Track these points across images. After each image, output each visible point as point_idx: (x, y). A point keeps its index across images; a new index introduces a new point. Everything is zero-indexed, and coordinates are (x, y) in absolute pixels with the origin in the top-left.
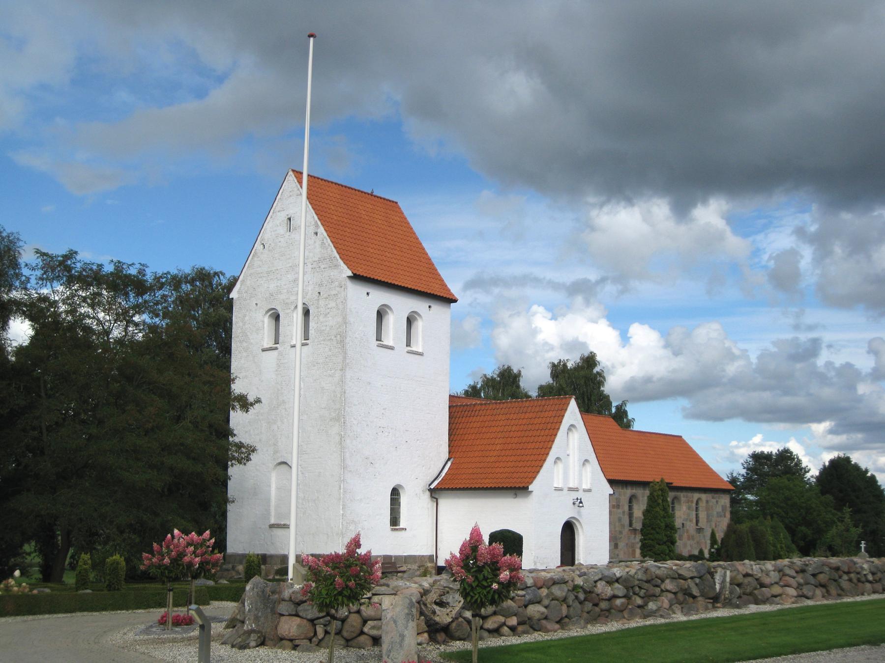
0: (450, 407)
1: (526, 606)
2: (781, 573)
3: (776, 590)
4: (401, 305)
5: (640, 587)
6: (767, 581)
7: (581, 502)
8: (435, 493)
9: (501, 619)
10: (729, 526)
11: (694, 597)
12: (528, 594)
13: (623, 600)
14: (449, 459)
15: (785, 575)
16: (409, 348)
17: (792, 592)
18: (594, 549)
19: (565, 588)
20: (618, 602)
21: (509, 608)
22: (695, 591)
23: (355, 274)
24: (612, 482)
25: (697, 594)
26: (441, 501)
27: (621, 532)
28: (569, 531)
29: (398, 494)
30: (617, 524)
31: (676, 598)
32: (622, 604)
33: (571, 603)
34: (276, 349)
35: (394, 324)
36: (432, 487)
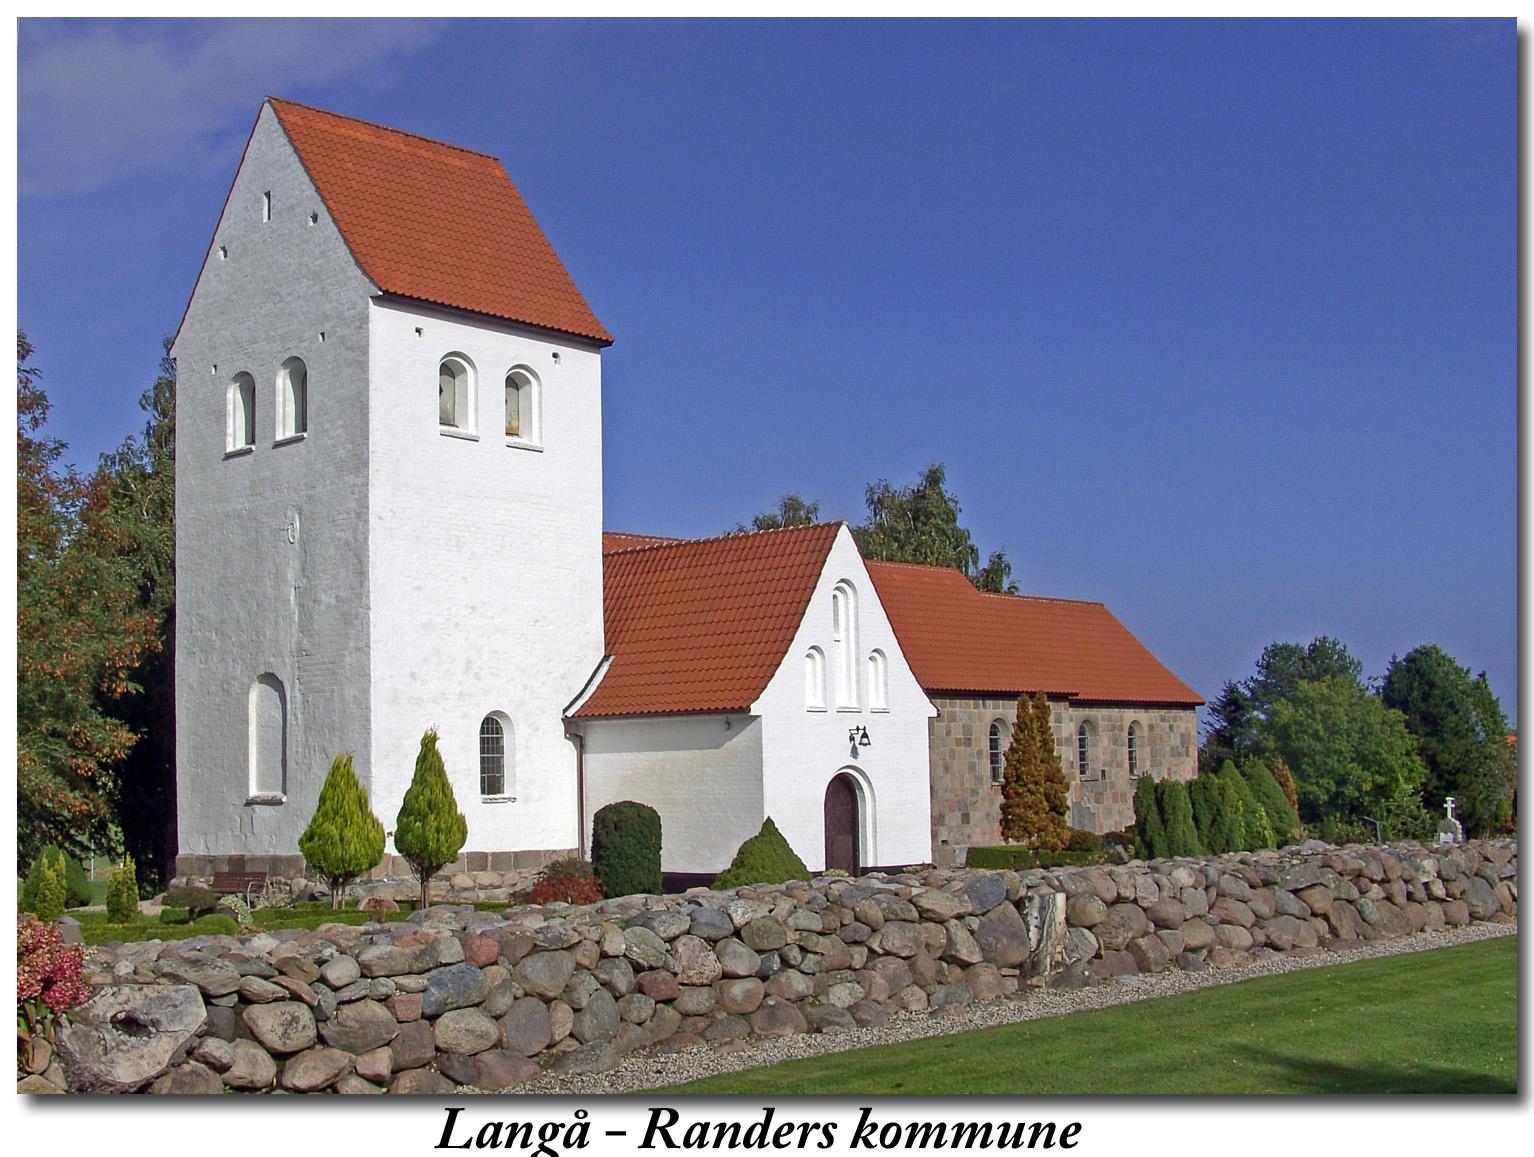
0: (604, 556)
1: (432, 1018)
2: (1213, 892)
3: (1201, 935)
4: (493, 352)
5: (803, 950)
6: (1172, 911)
7: (865, 735)
8: (576, 727)
9: (340, 1057)
10: (281, 857)
11: (965, 965)
12: (439, 984)
13: (749, 984)
14: (606, 658)
15: (1221, 895)
16: (512, 440)
17: (1242, 937)
18: (899, 832)
19: (567, 961)
20: (737, 989)
21: (364, 1024)
22: (968, 950)
23: (386, 292)
24: (932, 694)
25: (976, 958)
26: (591, 741)
27: (974, 792)
28: (844, 794)
29: (499, 730)
30: (967, 776)
31: (912, 967)
32: (748, 995)
33: (584, 1001)
34: (250, 451)
35: (484, 391)
36: (570, 714)
